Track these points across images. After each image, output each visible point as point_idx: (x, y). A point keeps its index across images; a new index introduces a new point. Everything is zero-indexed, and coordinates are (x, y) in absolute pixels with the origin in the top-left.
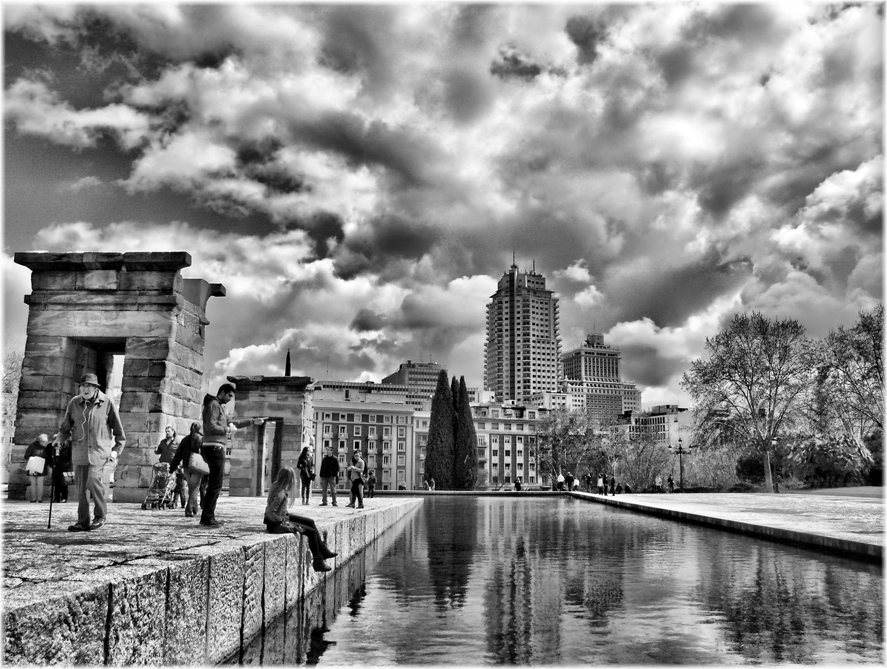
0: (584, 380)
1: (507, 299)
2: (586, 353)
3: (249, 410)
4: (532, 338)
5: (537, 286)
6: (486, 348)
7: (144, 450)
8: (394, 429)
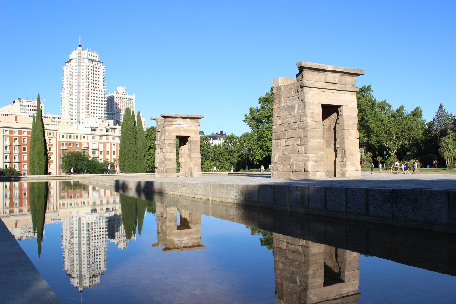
0: (115, 113)
1: (77, 64)
2: (117, 97)
3: (174, 132)
7: (355, 155)
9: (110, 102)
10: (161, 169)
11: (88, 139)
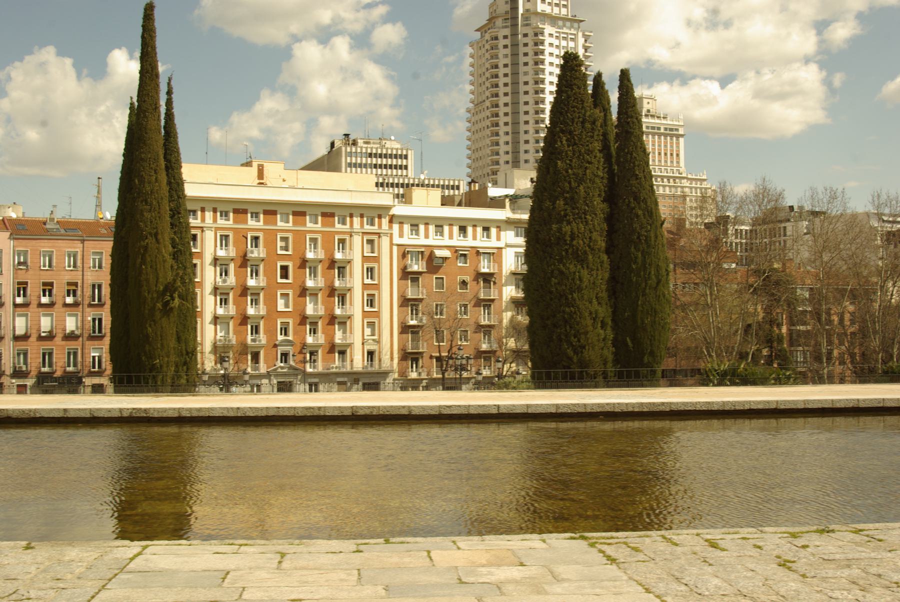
11: (498, 239)
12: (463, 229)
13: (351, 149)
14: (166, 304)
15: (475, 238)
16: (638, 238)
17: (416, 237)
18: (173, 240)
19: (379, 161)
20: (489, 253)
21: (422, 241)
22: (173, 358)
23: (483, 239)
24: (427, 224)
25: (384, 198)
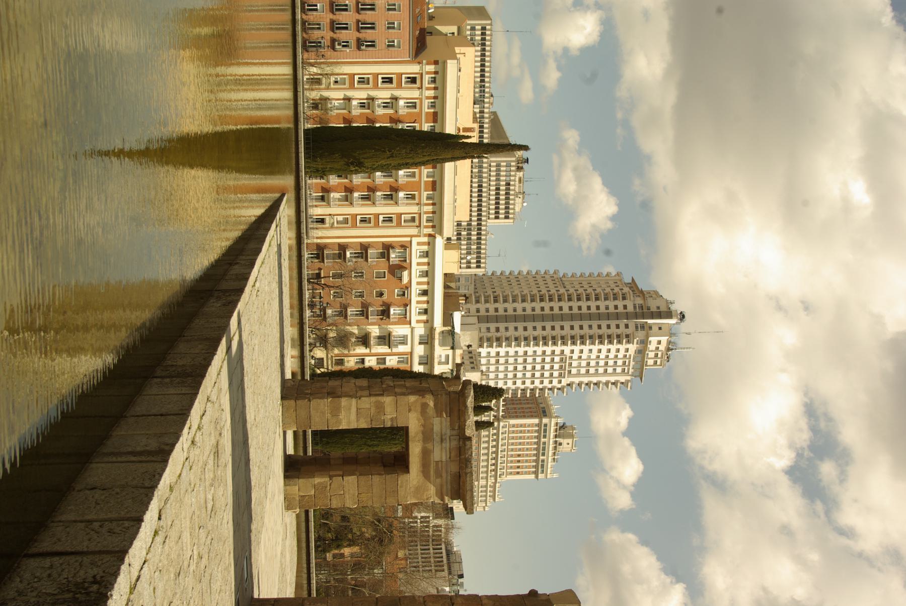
0: (502, 424)
1: (630, 309)
2: (546, 425)
4: (567, 349)
5: (651, 355)
6: (552, 272)
8: (415, 209)
9: (530, 408)
10: (308, 389)
11: (418, 322)
12: (425, 293)
13: (513, 166)
14: (352, 163)
15: (418, 302)
16: (395, 434)
17: (418, 256)
18: (391, 164)
19: (502, 193)
20: (406, 315)
21: (415, 260)
22: (320, 166)
23: (417, 309)
24: (428, 264)
25: (449, 229)
